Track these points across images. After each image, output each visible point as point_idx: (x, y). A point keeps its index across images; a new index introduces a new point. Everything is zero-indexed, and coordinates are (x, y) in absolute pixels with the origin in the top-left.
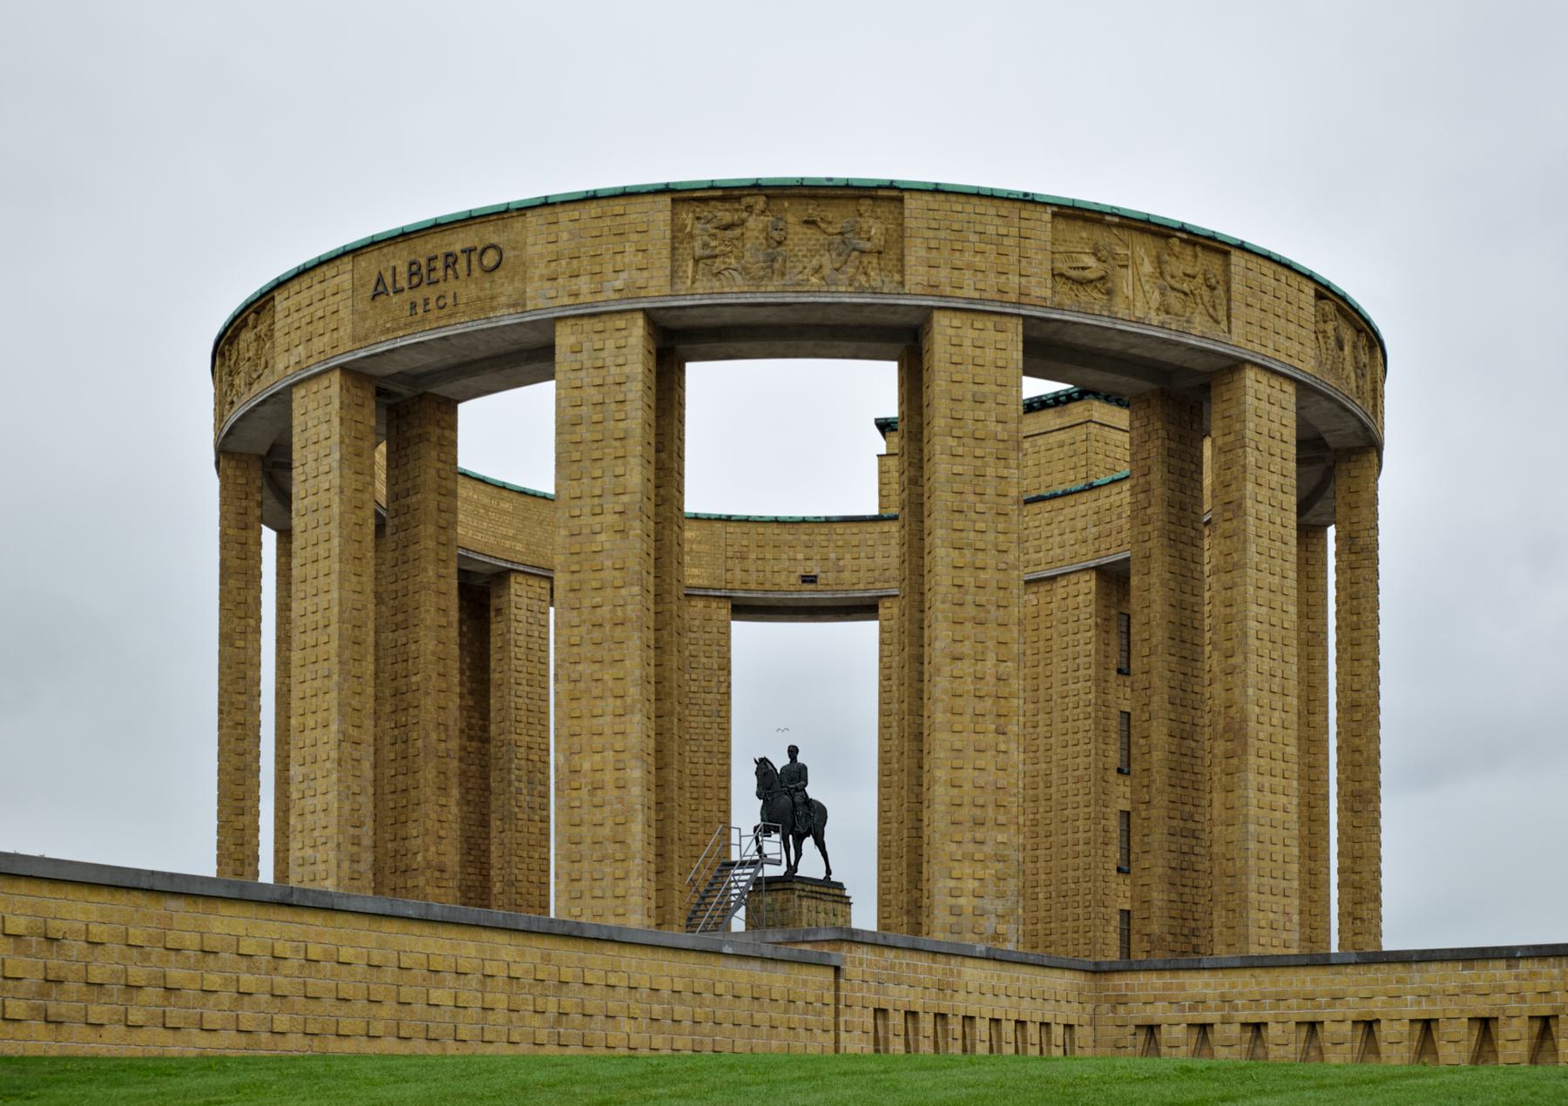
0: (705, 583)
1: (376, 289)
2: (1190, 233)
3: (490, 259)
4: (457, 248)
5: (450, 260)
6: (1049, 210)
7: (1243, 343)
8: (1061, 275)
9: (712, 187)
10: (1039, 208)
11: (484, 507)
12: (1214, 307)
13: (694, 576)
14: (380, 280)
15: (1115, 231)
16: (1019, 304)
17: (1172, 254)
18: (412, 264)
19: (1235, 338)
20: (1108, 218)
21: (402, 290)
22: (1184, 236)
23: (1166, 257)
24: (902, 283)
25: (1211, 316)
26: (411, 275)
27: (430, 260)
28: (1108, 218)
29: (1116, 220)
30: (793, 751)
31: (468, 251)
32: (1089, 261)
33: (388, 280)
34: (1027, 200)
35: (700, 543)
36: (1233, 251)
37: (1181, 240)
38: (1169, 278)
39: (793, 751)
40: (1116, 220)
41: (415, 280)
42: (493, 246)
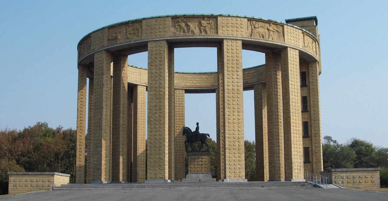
0: (256, 81)
2: (131, 21)
6: (107, 28)
7: (145, 38)
8: (109, 39)
10: (106, 29)
11: (207, 78)
12: (138, 34)
13: (254, 80)
15: (119, 27)
16: (102, 48)
17: (129, 27)
19: (143, 38)
20: (116, 25)
22: (131, 22)
23: (128, 28)
25: (137, 36)
28: (116, 25)
29: (117, 25)
30: (198, 124)
32: (114, 35)
34: (104, 28)
35: (255, 73)
36: (143, 21)
37: (131, 23)
38: (128, 32)
39: (198, 124)
40: (117, 25)
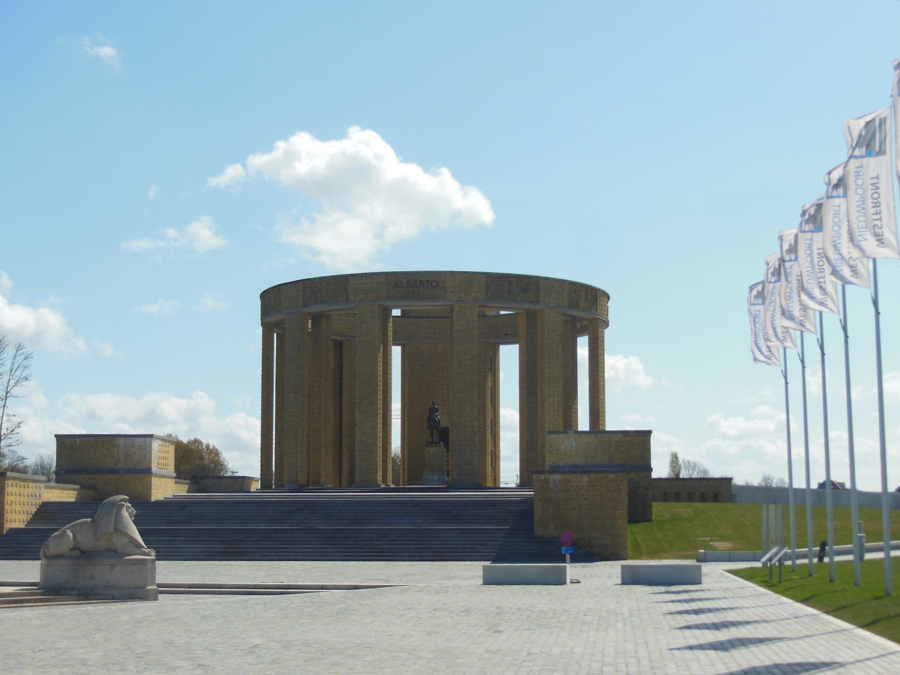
1: (395, 286)
3: (434, 284)
4: (424, 279)
5: (421, 283)
9: (497, 274)
14: (396, 283)
18: (408, 281)
21: (404, 288)
24: (538, 302)
26: (408, 284)
27: (414, 281)
31: (427, 281)
32: (574, 296)
33: (399, 284)
41: (409, 286)
42: (436, 281)
